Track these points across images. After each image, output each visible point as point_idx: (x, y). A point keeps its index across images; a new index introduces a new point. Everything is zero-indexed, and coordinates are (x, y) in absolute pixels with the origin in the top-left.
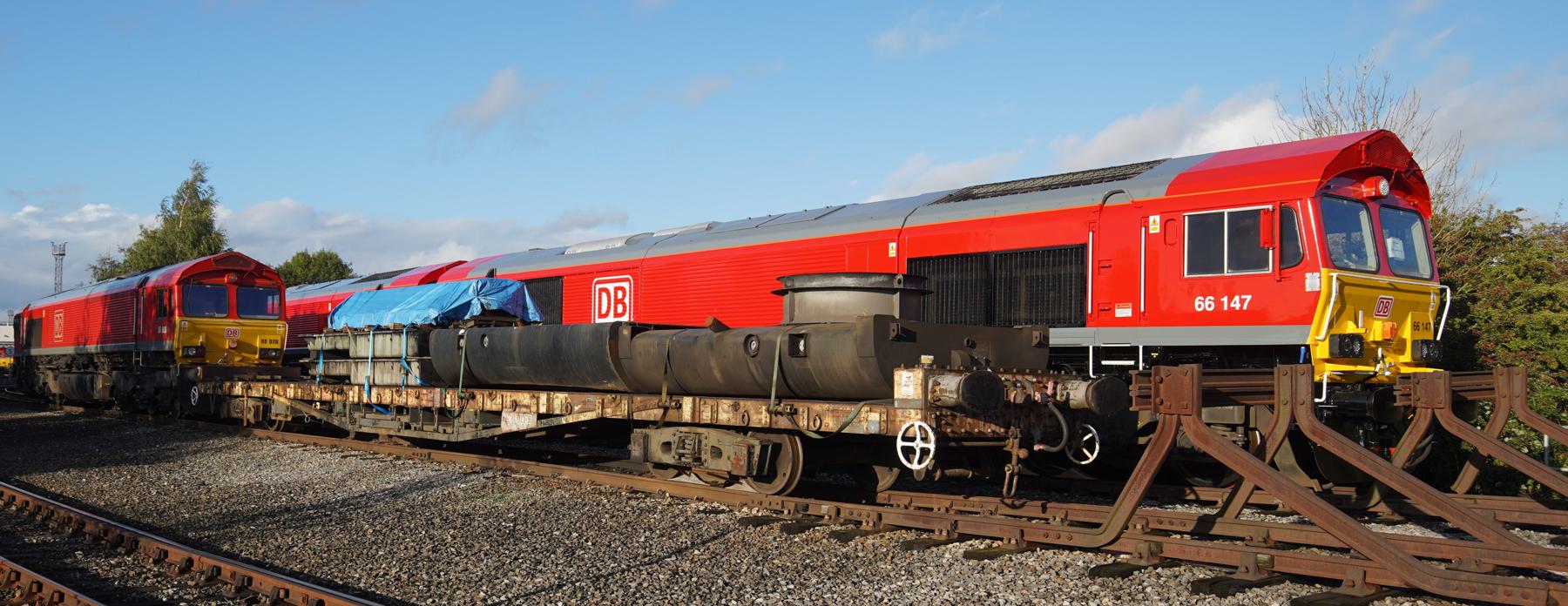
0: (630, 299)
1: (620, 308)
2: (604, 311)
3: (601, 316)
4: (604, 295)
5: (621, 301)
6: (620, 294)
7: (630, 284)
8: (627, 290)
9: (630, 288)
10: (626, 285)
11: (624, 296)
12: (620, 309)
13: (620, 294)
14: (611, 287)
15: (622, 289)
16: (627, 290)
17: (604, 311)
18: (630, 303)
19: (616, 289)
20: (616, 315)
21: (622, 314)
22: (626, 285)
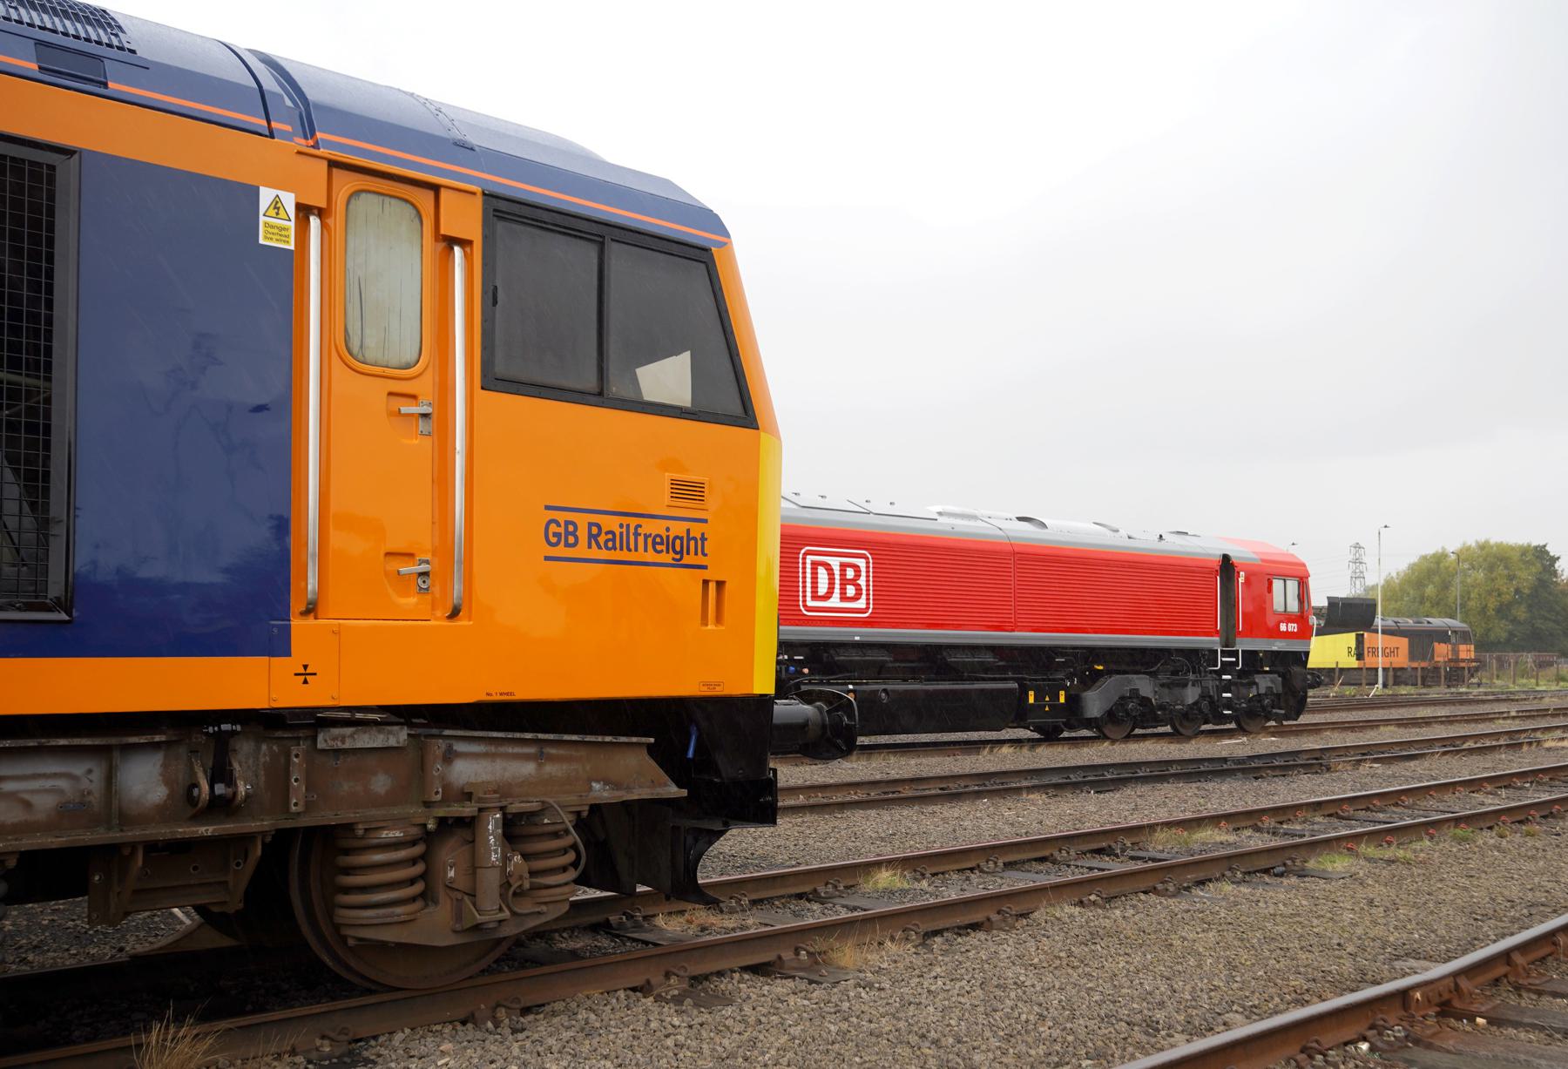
0: (868, 581)
1: (851, 591)
2: (822, 590)
3: (815, 597)
4: (822, 571)
5: (854, 582)
6: (850, 573)
7: (868, 563)
8: (863, 570)
9: (868, 567)
10: (861, 563)
11: (858, 575)
12: (851, 591)
13: (850, 573)
14: (835, 562)
15: (857, 568)
16: (863, 570)
17: (822, 590)
18: (868, 585)
19: (843, 566)
20: (844, 598)
21: (856, 598)
22: (861, 563)
